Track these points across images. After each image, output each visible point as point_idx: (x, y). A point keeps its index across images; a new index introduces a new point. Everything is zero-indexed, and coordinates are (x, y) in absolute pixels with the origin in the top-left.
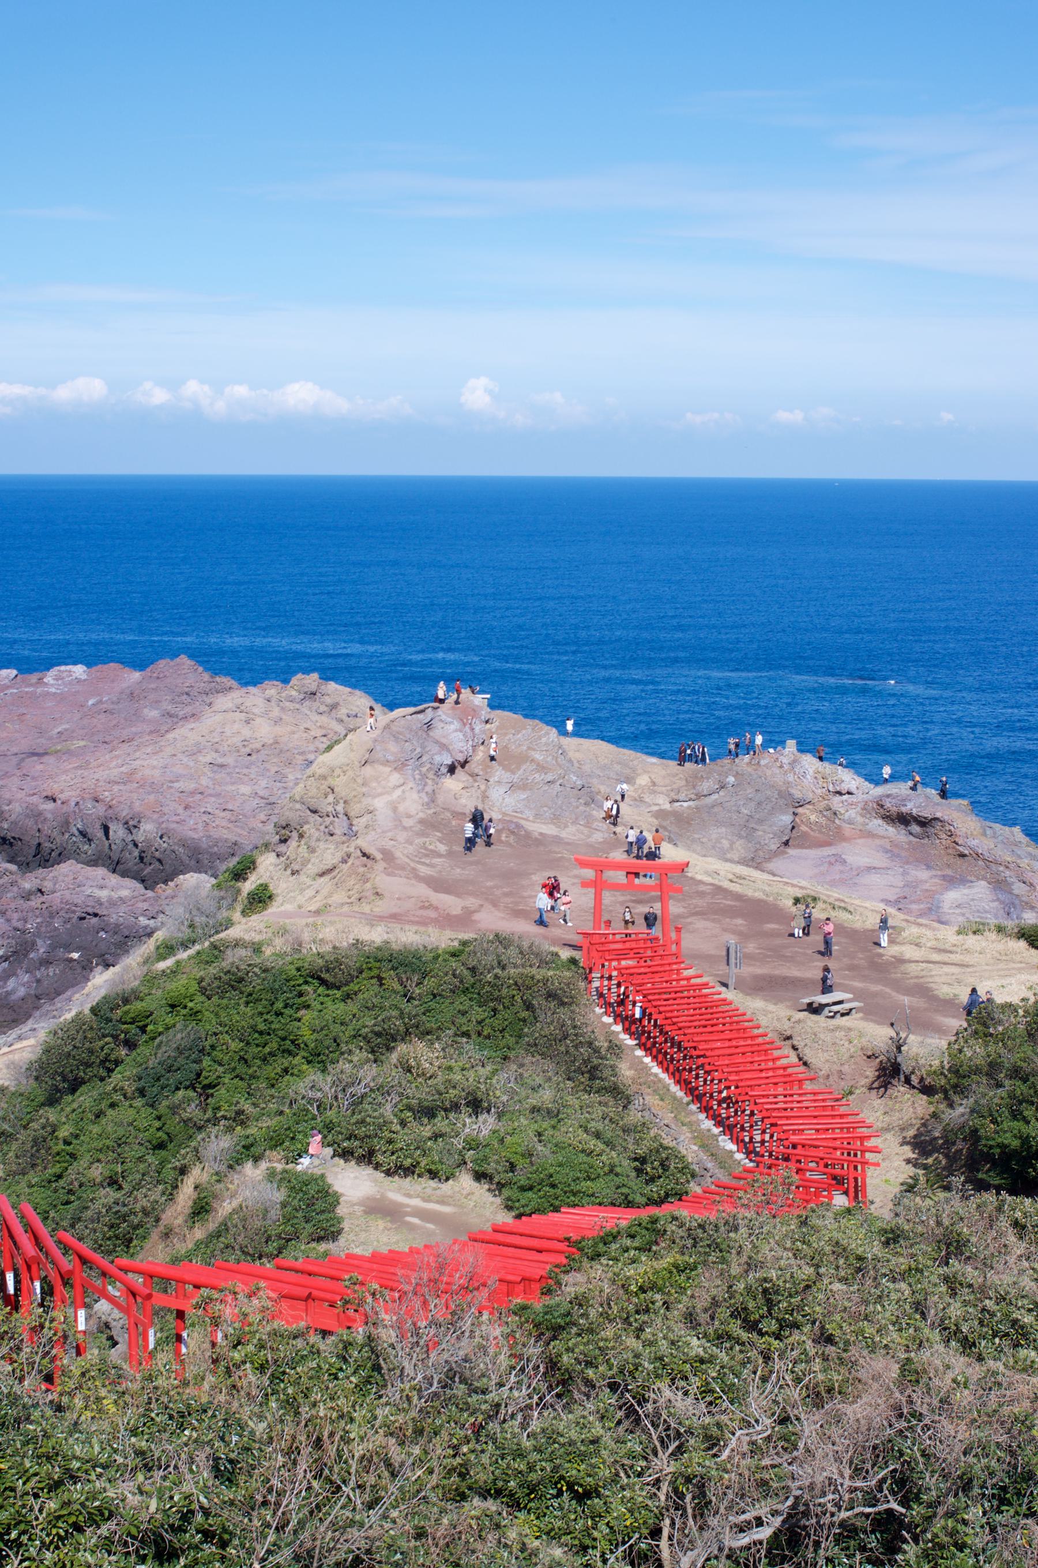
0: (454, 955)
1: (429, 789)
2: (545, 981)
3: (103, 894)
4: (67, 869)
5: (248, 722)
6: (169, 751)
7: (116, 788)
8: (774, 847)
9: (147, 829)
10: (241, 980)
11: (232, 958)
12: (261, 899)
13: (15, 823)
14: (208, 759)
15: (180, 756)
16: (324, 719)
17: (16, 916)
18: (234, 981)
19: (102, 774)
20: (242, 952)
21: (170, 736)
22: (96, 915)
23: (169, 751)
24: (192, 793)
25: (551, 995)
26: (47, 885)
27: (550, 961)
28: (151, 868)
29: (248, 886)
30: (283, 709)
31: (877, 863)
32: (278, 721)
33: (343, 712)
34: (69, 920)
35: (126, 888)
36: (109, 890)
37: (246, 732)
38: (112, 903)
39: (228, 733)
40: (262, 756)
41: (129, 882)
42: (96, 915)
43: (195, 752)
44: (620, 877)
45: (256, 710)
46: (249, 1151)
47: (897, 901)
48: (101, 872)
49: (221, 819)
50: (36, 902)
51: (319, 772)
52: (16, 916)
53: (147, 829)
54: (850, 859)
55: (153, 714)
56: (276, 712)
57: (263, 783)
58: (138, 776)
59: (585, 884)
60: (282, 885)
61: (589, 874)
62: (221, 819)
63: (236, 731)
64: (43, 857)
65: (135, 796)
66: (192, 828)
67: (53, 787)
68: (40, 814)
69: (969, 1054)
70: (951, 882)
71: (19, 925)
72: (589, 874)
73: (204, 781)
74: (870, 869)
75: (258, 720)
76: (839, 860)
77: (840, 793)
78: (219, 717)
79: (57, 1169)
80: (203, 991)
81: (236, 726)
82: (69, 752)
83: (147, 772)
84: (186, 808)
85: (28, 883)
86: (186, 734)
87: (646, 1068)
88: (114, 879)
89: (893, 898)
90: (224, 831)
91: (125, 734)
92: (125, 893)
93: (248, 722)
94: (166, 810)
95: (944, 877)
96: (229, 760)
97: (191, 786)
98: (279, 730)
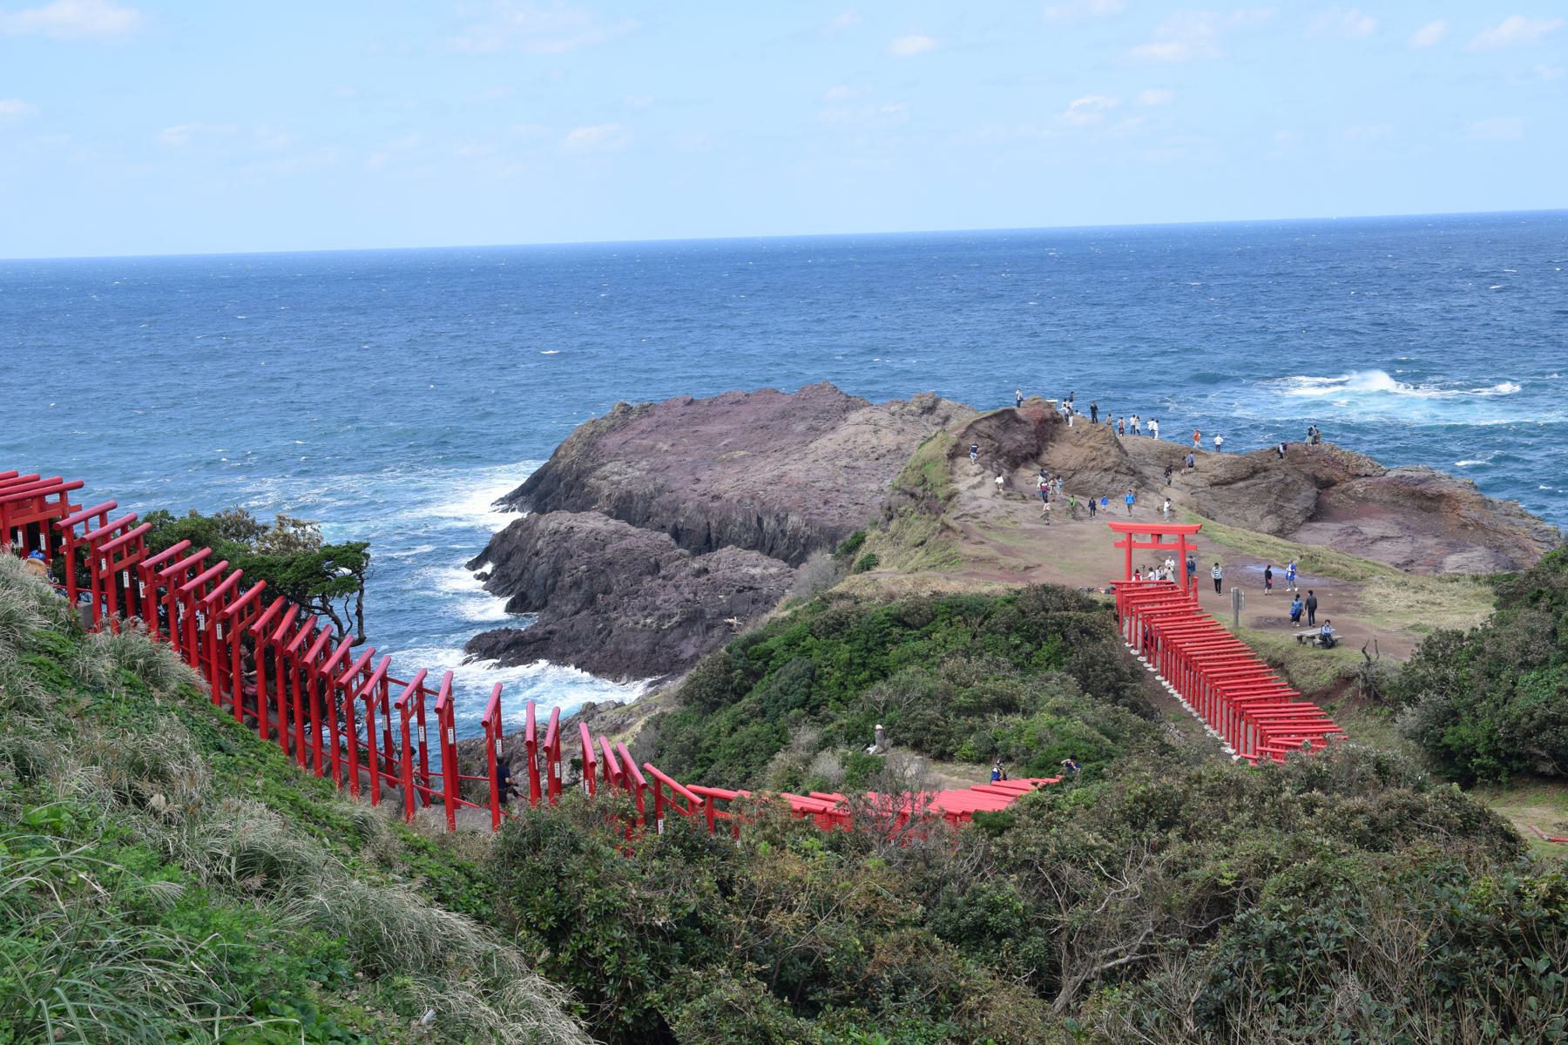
0: (1009, 602)
2: (1079, 621)
3: (757, 571)
4: (726, 553)
5: (875, 432)
6: (811, 457)
8: (1299, 520)
9: (794, 519)
10: (842, 624)
11: (835, 607)
12: (869, 564)
14: (844, 463)
18: (838, 626)
19: (759, 477)
20: (843, 604)
21: (812, 446)
22: (751, 588)
23: (811, 457)
24: (830, 491)
25: (1084, 631)
27: (1091, 606)
28: (794, 550)
29: (861, 555)
30: (904, 422)
31: (1389, 533)
32: (900, 432)
35: (775, 567)
36: (758, 567)
37: (874, 441)
38: (763, 578)
41: (775, 561)
42: (751, 588)
43: (833, 457)
46: (826, 743)
47: (1406, 564)
48: (755, 554)
49: (853, 511)
50: (703, 579)
53: (794, 519)
54: (1365, 530)
55: (800, 427)
56: (899, 424)
58: (786, 479)
59: (1117, 545)
60: (884, 552)
62: (853, 511)
63: (867, 439)
64: (708, 543)
67: (716, 488)
69: (1421, 672)
70: (1454, 547)
71: (691, 596)
73: (840, 481)
74: (1383, 538)
76: (1356, 531)
77: (1358, 476)
78: (852, 429)
79: (700, 771)
80: (812, 632)
81: (867, 436)
82: (733, 461)
83: (794, 474)
84: (826, 503)
85: (697, 564)
86: (825, 444)
87: (1164, 690)
88: (766, 561)
89: (1401, 561)
91: (778, 444)
92: (773, 570)
93: (875, 432)
94: (808, 505)
95: (1449, 544)
96: (861, 463)
97: (830, 485)
98: (900, 438)
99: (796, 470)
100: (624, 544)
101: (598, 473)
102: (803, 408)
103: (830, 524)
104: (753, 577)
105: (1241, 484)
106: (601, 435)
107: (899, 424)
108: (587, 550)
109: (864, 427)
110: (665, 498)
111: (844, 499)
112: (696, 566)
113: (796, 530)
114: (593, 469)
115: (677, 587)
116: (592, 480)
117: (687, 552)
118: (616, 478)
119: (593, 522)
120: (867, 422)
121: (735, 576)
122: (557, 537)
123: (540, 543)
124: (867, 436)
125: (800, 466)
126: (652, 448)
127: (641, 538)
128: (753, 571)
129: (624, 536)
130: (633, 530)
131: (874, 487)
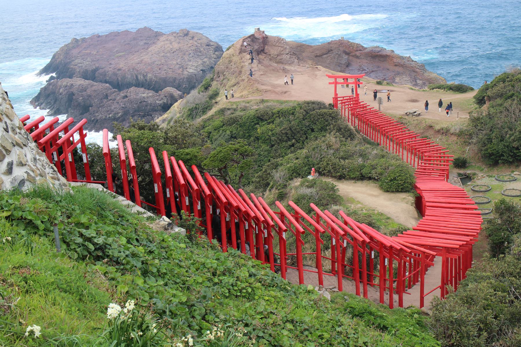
1: (258, 58)
3: (145, 95)
7: (138, 65)
9: (149, 75)
13: (110, 77)
14: (162, 54)
15: (154, 55)
16: (191, 41)
17: (122, 104)
18: (233, 121)
21: (149, 49)
26: (128, 94)
30: (179, 39)
32: (179, 43)
33: (196, 39)
34: (137, 104)
35: (151, 93)
37: (171, 47)
38: (148, 97)
39: (166, 47)
40: (177, 53)
44: (342, 81)
45: (172, 40)
48: (142, 89)
49: (170, 72)
50: (126, 99)
51: (227, 56)
52: (122, 104)
53: (149, 75)
57: (179, 60)
58: (144, 62)
61: (333, 80)
65: (144, 67)
66: (163, 74)
68: (117, 75)
72: (333, 80)
73: (163, 61)
75: (174, 43)
78: (162, 43)
81: (168, 45)
83: (146, 60)
84: (160, 69)
85: (122, 94)
88: (147, 91)
90: (171, 75)
92: (151, 94)
94: (154, 70)
96: (168, 55)
98: (180, 45)
99: (146, 58)
100: (93, 88)
101: (73, 63)
102: (141, 37)
103: (163, 76)
104: (144, 97)
105: (325, 56)
106: (70, 50)
107: (178, 41)
108: (80, 92)
109: (166, 42)
110: (101, 71)
111: (165, 67)
112: (123, 95)
113: (151, 79)
114: (70, 62)
115: (118, 103)
116: (72, 66)
117: (117, 90)
118: (80, 65)
119: (79, 82)
120: (167, 40)
121: (138, 97)
122: (67, 88)
123: (61, 90)
124: (168, 45)
125: (147, 57)
126: (90, 53)
127: (98, 86)
128: (143, 95)
129: (92, 86)
130: (95, 83)
131: (175, 62)
